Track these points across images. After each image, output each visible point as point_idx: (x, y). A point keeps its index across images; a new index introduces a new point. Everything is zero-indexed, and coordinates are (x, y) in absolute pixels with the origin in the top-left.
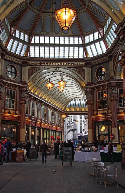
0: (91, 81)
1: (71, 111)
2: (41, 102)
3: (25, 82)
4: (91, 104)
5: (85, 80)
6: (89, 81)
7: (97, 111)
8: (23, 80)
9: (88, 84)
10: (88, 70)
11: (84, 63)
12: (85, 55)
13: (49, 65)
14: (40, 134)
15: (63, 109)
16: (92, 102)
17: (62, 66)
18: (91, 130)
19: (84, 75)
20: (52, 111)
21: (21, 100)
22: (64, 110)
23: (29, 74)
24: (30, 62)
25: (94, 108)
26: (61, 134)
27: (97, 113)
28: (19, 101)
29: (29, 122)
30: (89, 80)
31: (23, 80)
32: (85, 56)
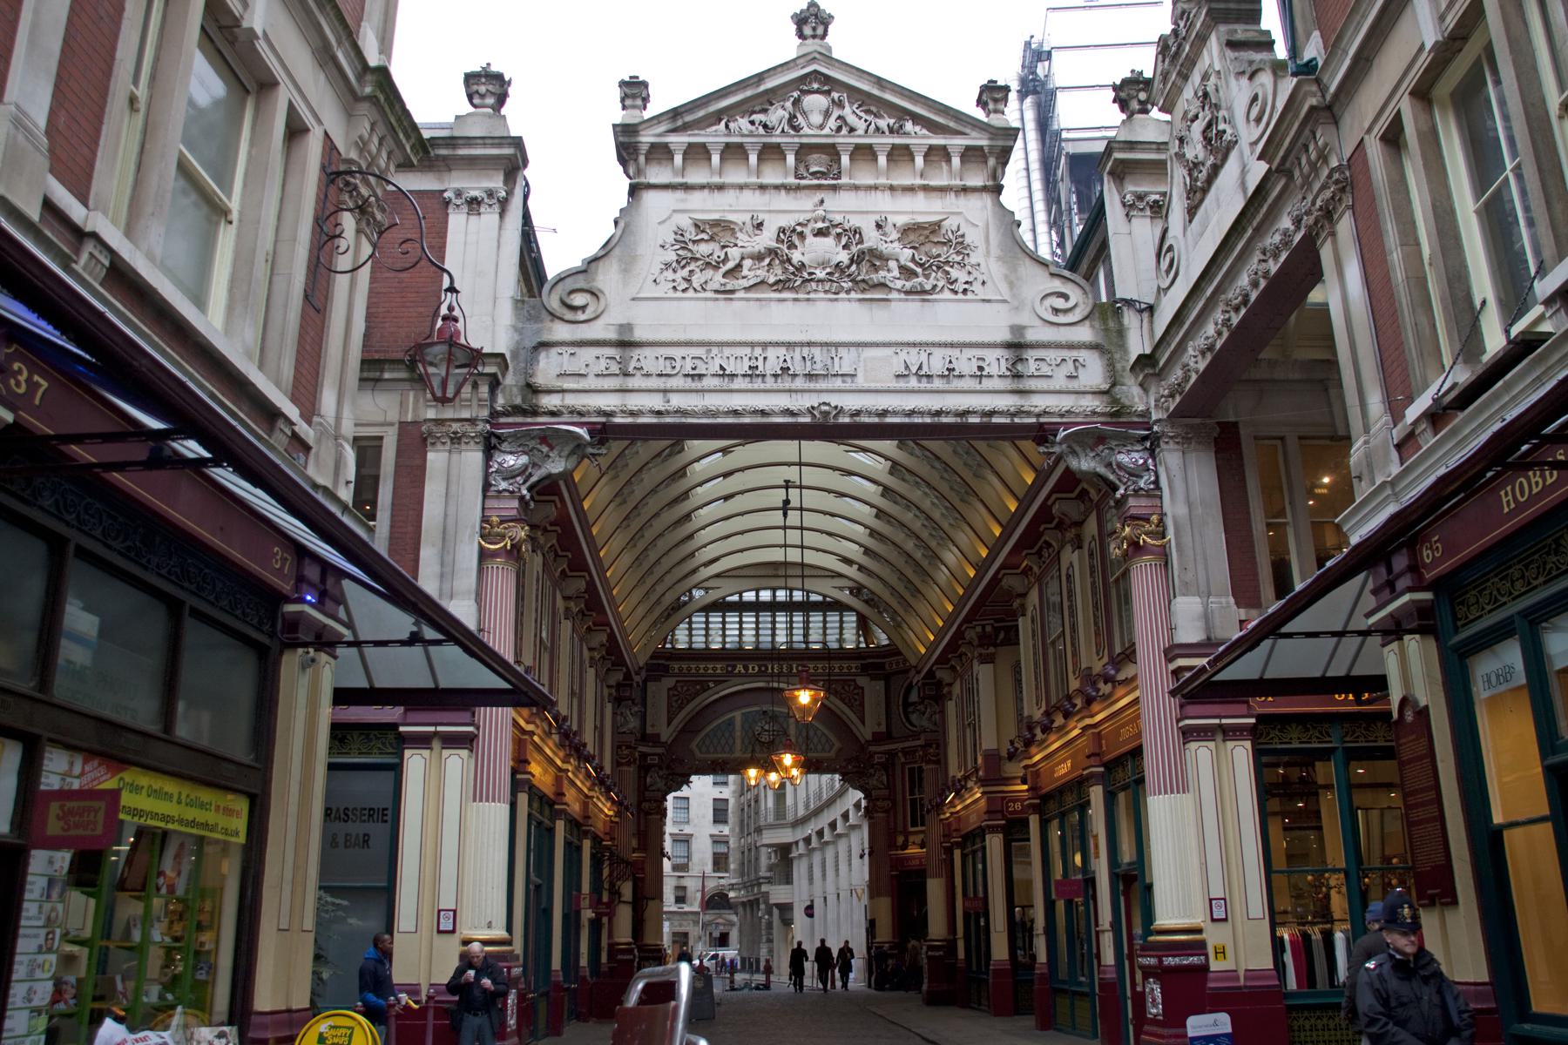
0: (883, 728)
3: (658, 735)
4: (887, 811)
5: (863, 723)
6: (876, 729)
7: (907, 834)
8: (649, 730)
9: (878, 738)
10: (873, 691)
12: (862, 639)
13: (740, 675)
16: (887, 804)
19: (862, 705)
21: (645, 801)
23: (670, 706)
24: (676, 666)
25: (895, 823)
27: (906, 840)
28: (639, 805)
30: (879, 724)
31: (649, 730)
32: (863, 645)
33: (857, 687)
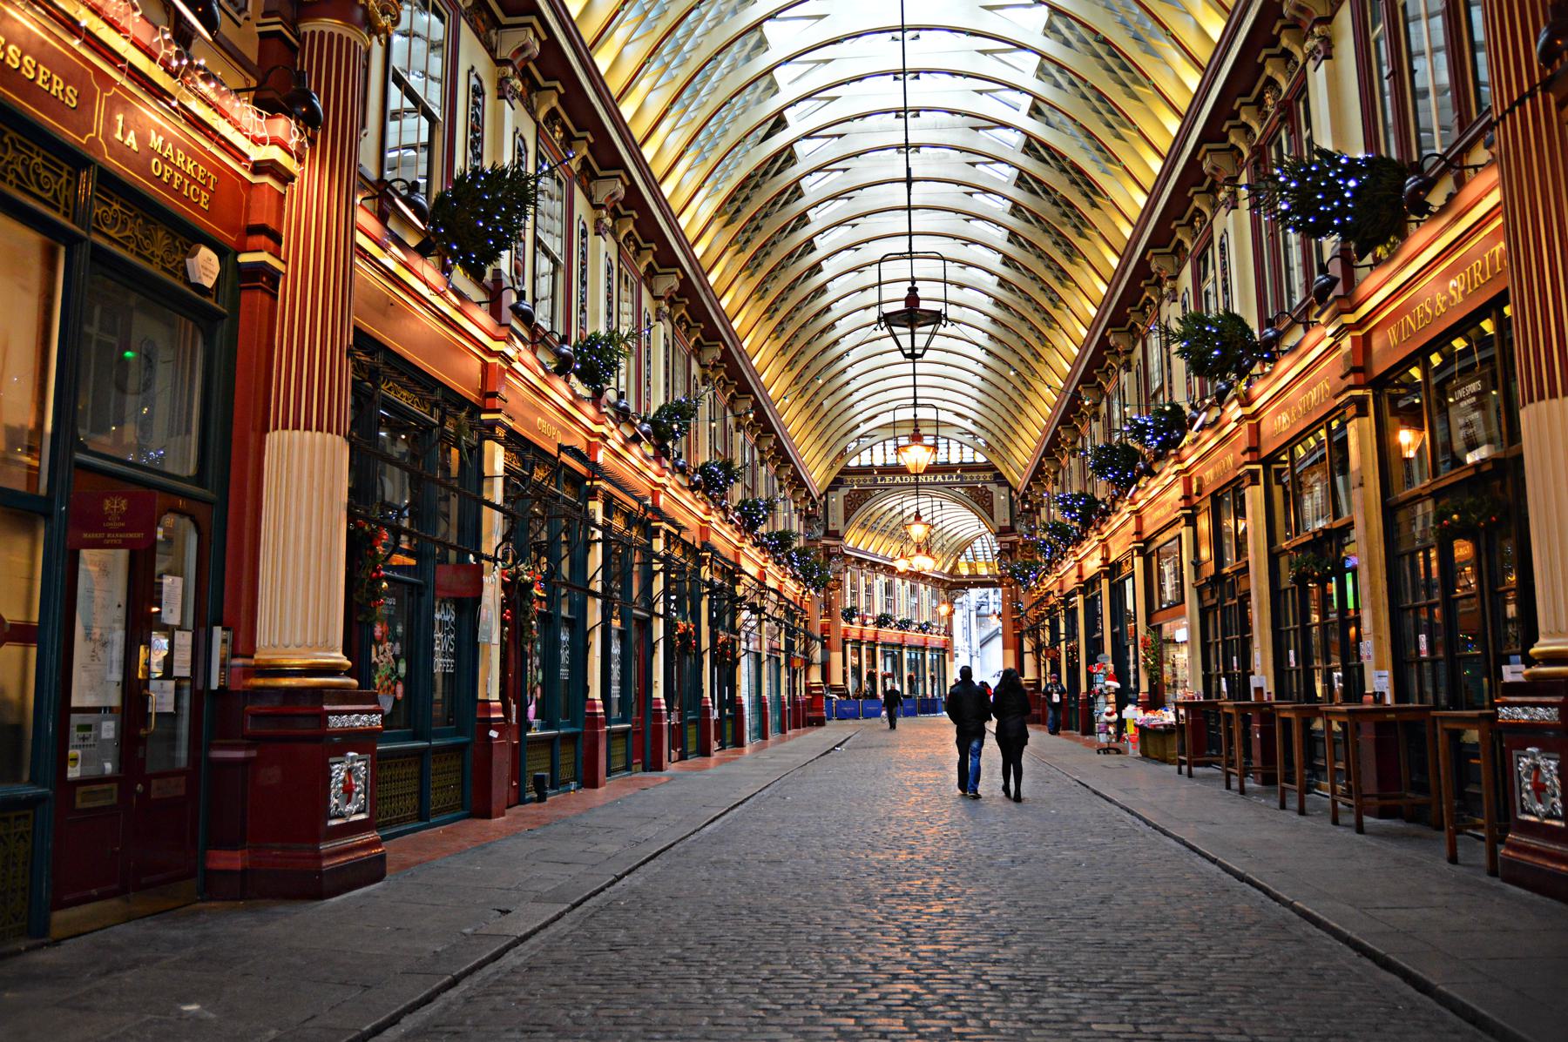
0: (1008, 523)
1: (977, 575)
2: (874, 565)
6: (1002, 524)
8: (831, 528)
11: (989, 474)
13: (898, 485)
14: (874, 665)
15: (946, 570)
17: (931, 484)
18: (1011, 653)
19: (992, 505)
20: (908, 583)
22: (951, 573)
23: (846, 508)
26: (944, 657)
29: (846, 631)
31: (831, 528)
33: (987, 492)
